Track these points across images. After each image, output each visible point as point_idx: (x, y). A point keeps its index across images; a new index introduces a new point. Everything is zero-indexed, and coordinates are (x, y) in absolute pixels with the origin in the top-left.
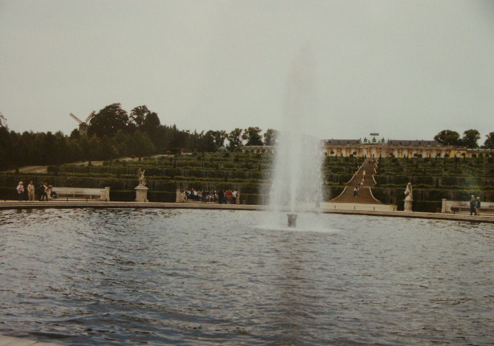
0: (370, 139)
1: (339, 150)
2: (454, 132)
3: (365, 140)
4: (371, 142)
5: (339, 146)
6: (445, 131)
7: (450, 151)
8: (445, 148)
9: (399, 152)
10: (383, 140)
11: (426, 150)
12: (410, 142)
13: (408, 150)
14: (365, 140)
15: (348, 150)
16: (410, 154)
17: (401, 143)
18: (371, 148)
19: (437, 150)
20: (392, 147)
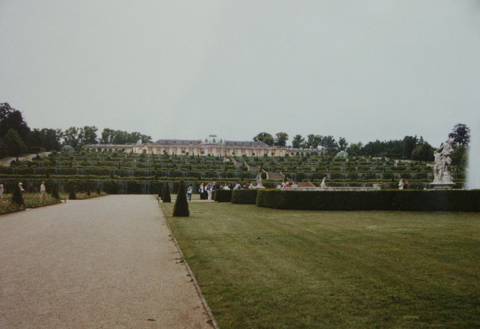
0: (210, 140)
3: (206, 140)
4: (212, 143)
6: (262, 133)
7: (275, 150)
8: (272, 148)
10: (221, 141)
11: (257, 150)
12: (243, 143)
13: (242, 149)
14: (206, 140)
15: (191, 149)
17: (235, 143)
18: (211, 148)
19: (265, 150)
20: (228, 147)
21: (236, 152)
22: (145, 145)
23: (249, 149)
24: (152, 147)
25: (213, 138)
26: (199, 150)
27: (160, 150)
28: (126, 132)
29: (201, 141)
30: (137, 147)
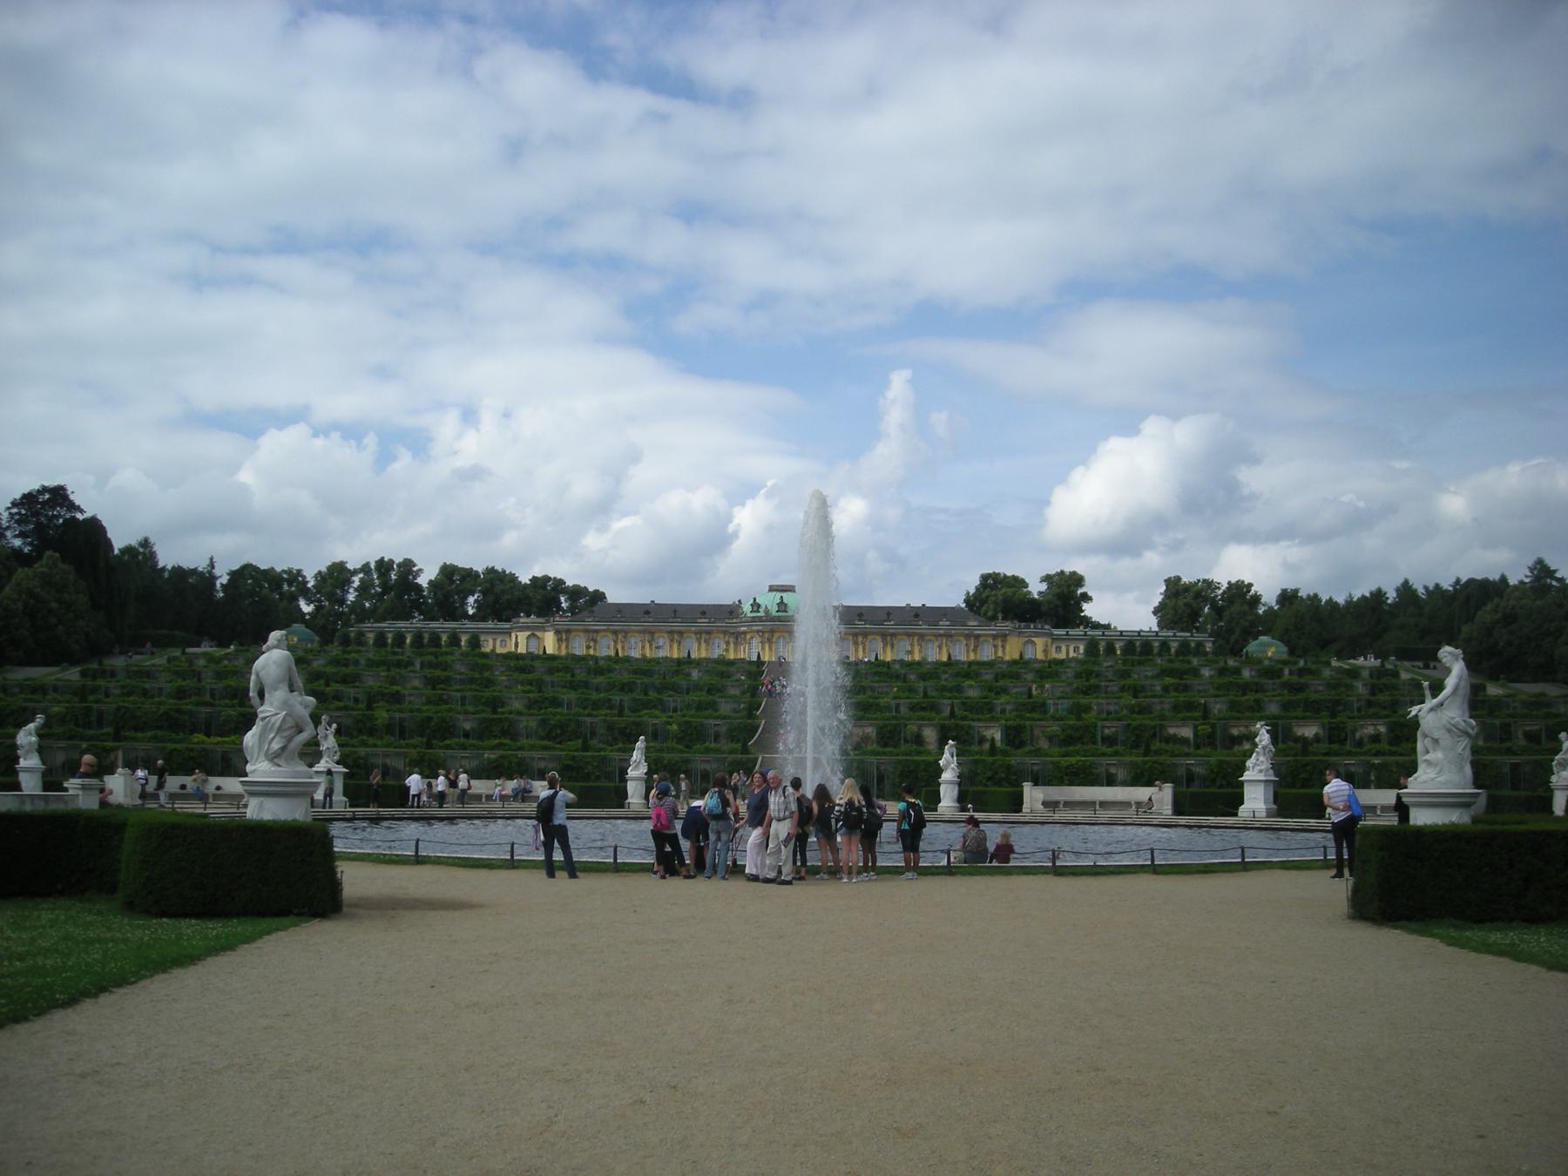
0: (769, 601)
2: (1015, 578)
3: (756, 606)
4: (774, 612)
5: (677, 626)
7: (1004, 637)
8: (993, 629)
9: (856, 643)
12: (889, 612)
13: (884, 636)
18: (772, 632)
19: (967, 637)
23: (910, 635)
24: (568, 631)
27: (595, 641)
28: (513, 578)
30: (522, 629)
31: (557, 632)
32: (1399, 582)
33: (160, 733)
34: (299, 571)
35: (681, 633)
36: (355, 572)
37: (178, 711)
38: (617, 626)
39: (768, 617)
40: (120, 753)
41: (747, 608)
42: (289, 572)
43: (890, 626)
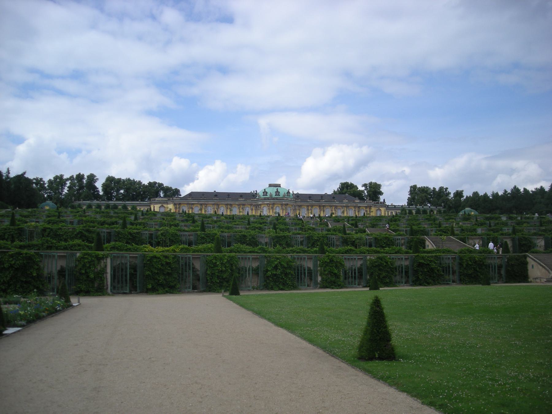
1: (229, 207)
4: (274, 196)
7: (370, 207)
9: (308, 210)
10: (288, 192)
13: (320, 206)
14: (265, 193)
16: (322, 212)
18: (274, 204)
19: (355, 207)
21: (311, 210)
22: (169, 200)
23: (331, 206)
24: (180, 204)
25: (275, 189)
26: (254, 208)
27: (192, 208)
28: (140, 183)
29: (256, 193)
30: (157, 203)
31: (175, 204)
32: (512, 187)
33: (119, 244)
34: (41, 179)
35: (231, 205)
36: (67, 180)
37: (88, 231)
38: (202, 202)
39: (271, 198)
40: (109, 260)
41: (261, 194)
42: (37, 179)
43: (323, 202)
